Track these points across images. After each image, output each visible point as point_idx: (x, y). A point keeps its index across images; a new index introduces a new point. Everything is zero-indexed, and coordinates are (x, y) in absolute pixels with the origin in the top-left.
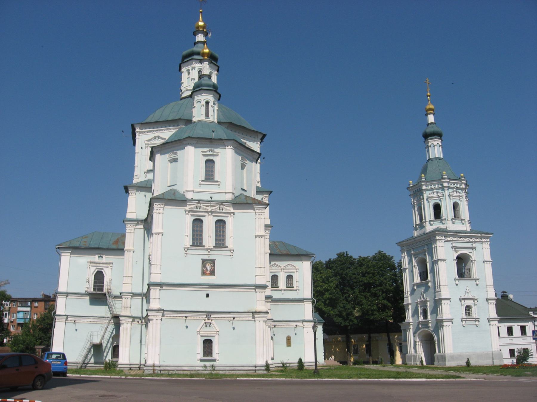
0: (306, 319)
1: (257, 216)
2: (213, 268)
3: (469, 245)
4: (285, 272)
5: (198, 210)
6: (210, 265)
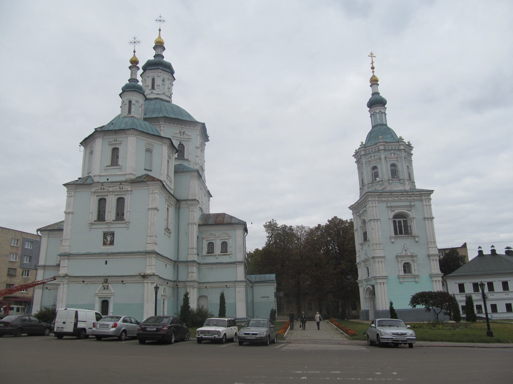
0: (238, 279)
1: (151, 192)
2: (112, 239)
3: (408, 204)
4: (220, 240)
5: (103, 191)
6: (110, 236)
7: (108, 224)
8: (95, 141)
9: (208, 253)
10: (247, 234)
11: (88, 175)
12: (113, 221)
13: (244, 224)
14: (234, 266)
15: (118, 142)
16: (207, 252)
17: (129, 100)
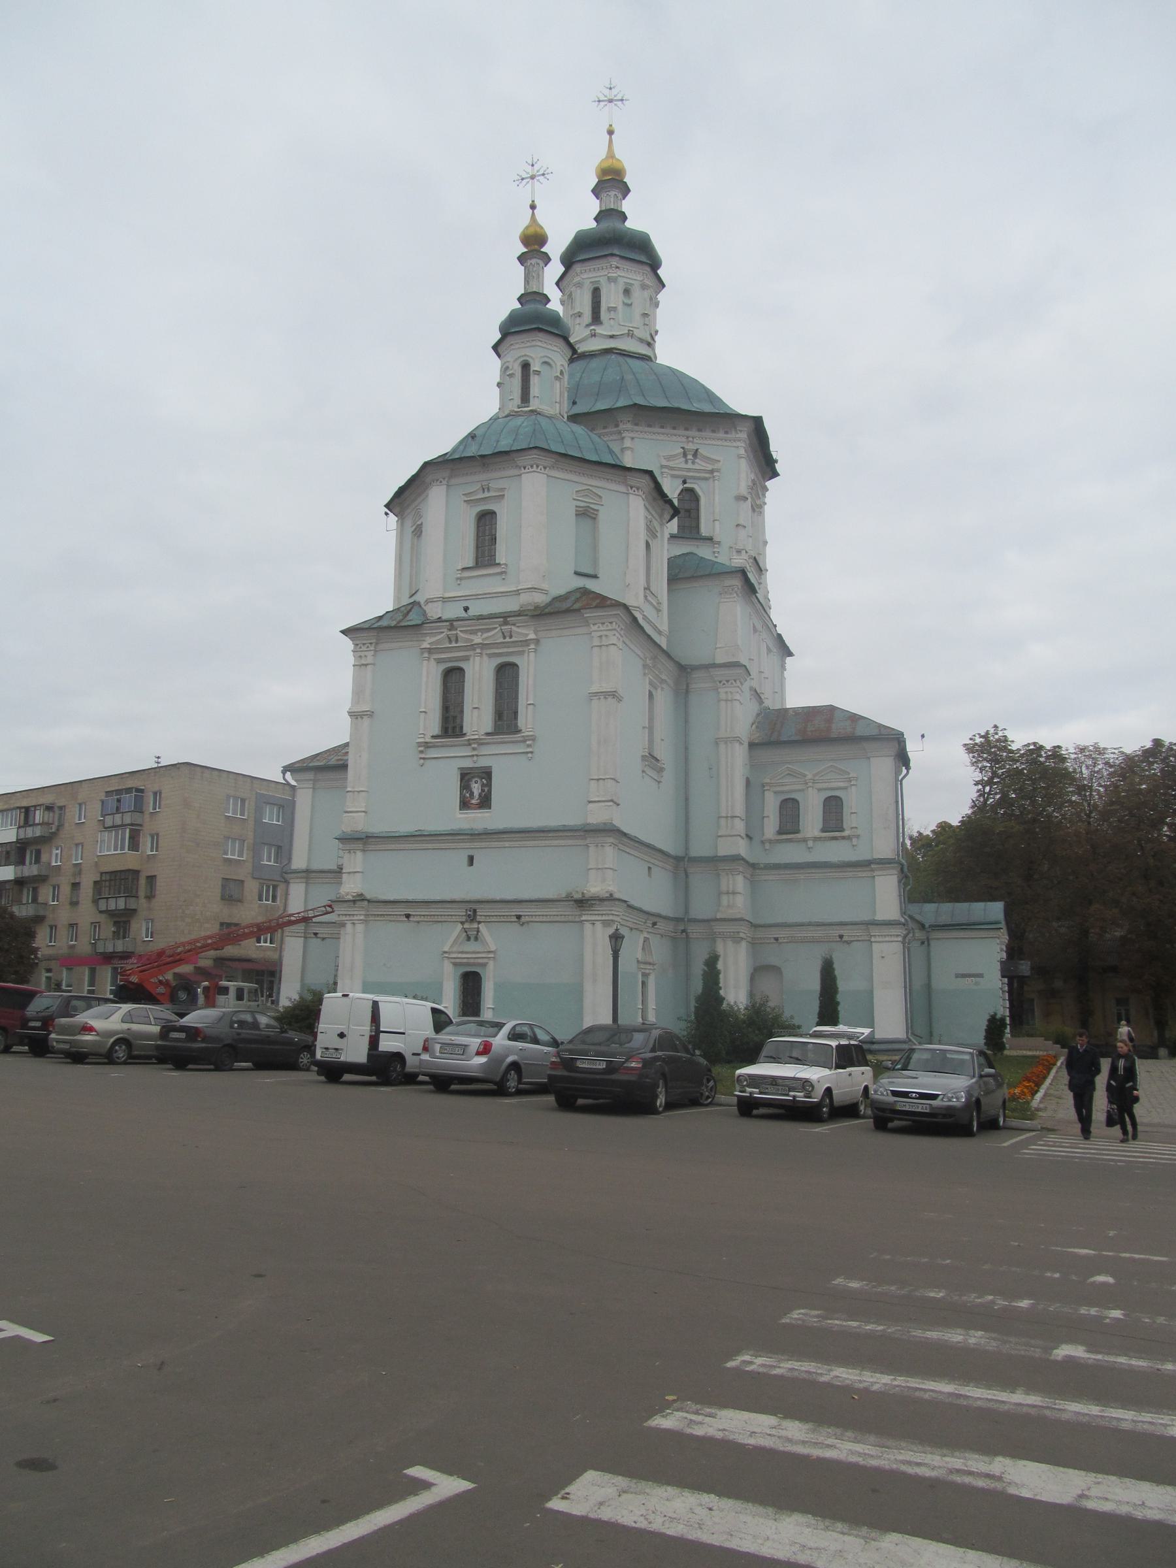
0: (880, 917)
1: (596, 642)
2: (486, 789)
4: (819, 790)
5: (454, 645)
7: (473, 746)
8: (427, 496)
9: (780, 832)
10: (908, 772)
11: (412, 600)
12: (488, 734)
13: (898, 739)
14: (864, 874)
15: (492, 494)
16: (778, 829)
17: (522, 359)
